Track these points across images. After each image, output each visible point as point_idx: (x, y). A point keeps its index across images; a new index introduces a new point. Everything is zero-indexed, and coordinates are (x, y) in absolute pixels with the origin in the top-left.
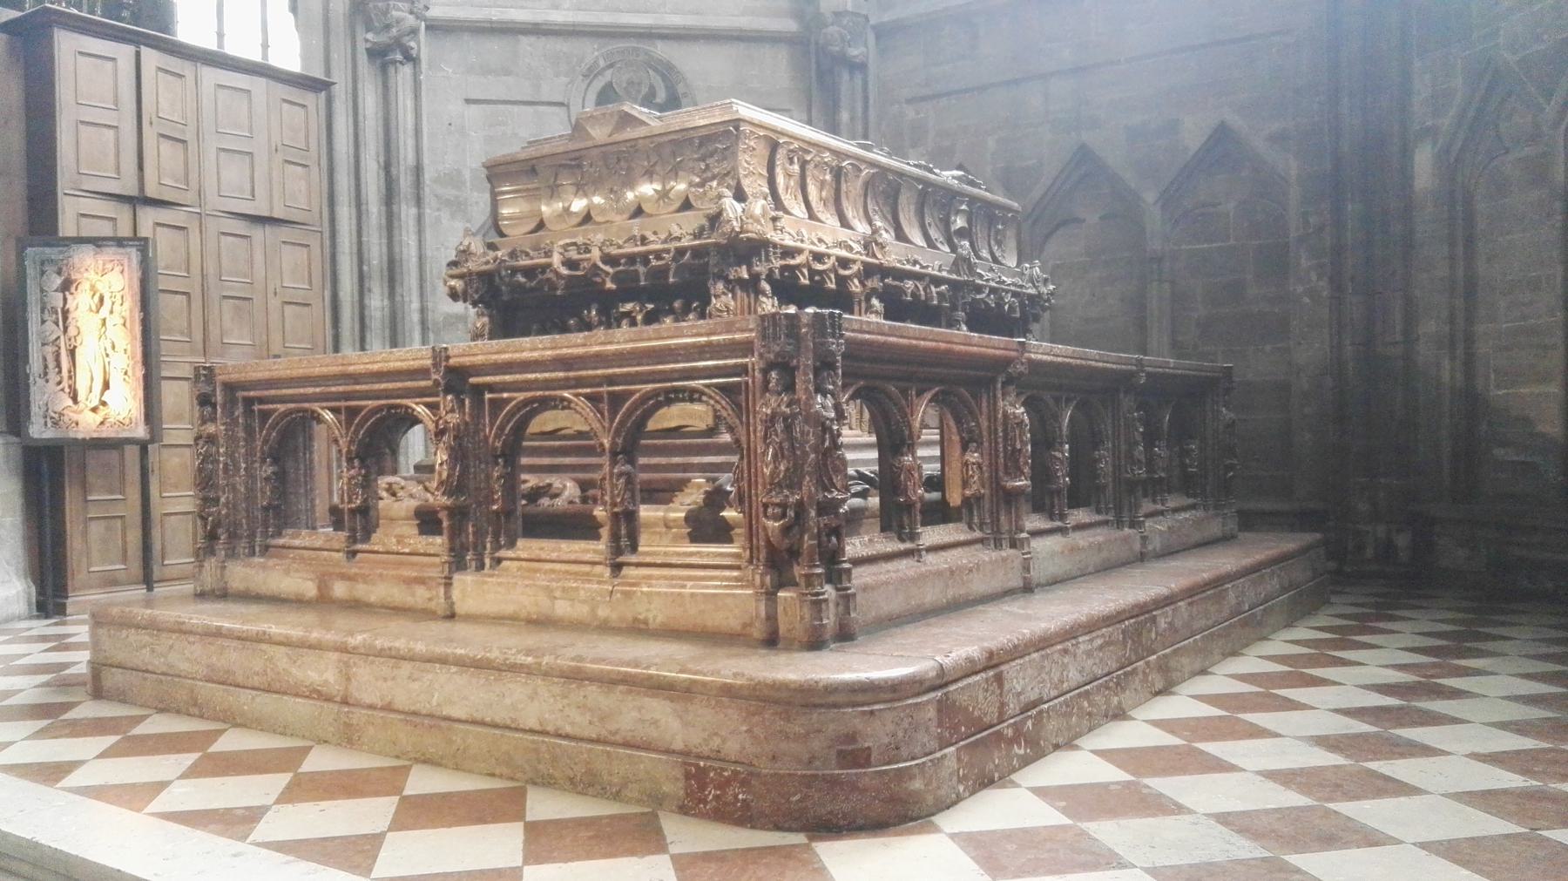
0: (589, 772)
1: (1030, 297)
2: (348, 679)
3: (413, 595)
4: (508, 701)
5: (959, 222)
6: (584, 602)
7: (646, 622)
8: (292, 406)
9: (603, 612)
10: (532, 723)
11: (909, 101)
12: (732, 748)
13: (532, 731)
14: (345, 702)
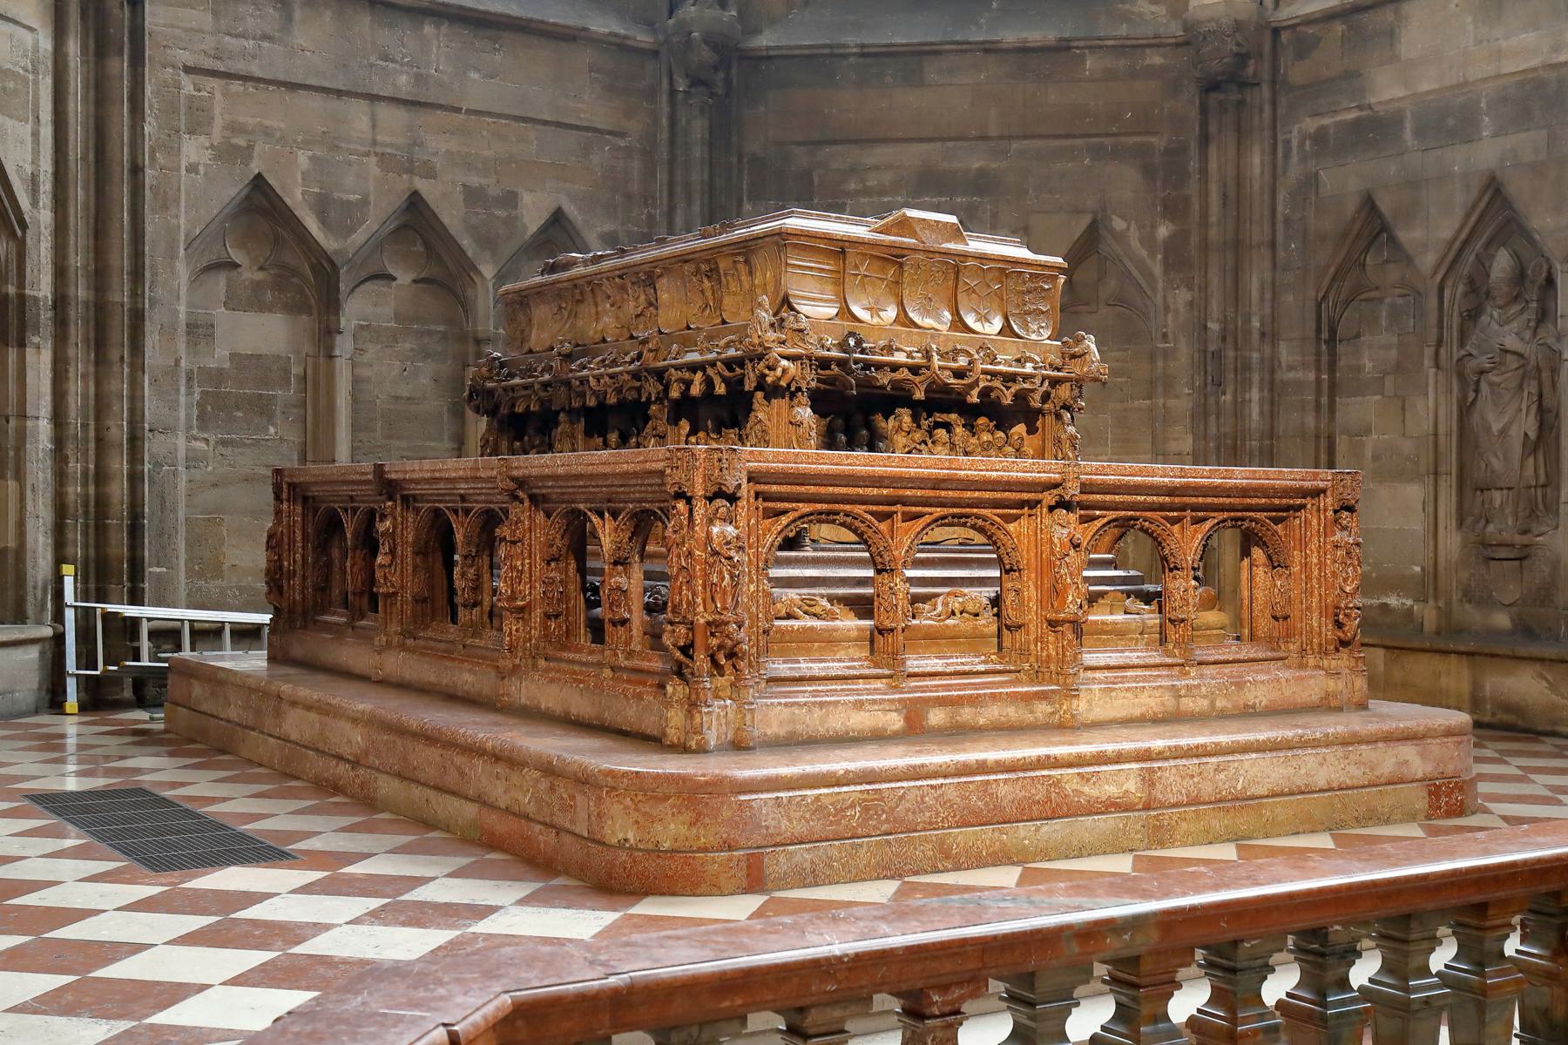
0: (1369, 810)
2: (1152, 784)
3: (1032, 712)
4: (1303, 771)
6: (1205, 697)
7: (1254, 707)
8: (819, 506)
9: (1219, 704)
10: (1322, 783)
11: (188, 70)
12: (1450, 769)
13: (1321, 791)
14: (1147, 808)
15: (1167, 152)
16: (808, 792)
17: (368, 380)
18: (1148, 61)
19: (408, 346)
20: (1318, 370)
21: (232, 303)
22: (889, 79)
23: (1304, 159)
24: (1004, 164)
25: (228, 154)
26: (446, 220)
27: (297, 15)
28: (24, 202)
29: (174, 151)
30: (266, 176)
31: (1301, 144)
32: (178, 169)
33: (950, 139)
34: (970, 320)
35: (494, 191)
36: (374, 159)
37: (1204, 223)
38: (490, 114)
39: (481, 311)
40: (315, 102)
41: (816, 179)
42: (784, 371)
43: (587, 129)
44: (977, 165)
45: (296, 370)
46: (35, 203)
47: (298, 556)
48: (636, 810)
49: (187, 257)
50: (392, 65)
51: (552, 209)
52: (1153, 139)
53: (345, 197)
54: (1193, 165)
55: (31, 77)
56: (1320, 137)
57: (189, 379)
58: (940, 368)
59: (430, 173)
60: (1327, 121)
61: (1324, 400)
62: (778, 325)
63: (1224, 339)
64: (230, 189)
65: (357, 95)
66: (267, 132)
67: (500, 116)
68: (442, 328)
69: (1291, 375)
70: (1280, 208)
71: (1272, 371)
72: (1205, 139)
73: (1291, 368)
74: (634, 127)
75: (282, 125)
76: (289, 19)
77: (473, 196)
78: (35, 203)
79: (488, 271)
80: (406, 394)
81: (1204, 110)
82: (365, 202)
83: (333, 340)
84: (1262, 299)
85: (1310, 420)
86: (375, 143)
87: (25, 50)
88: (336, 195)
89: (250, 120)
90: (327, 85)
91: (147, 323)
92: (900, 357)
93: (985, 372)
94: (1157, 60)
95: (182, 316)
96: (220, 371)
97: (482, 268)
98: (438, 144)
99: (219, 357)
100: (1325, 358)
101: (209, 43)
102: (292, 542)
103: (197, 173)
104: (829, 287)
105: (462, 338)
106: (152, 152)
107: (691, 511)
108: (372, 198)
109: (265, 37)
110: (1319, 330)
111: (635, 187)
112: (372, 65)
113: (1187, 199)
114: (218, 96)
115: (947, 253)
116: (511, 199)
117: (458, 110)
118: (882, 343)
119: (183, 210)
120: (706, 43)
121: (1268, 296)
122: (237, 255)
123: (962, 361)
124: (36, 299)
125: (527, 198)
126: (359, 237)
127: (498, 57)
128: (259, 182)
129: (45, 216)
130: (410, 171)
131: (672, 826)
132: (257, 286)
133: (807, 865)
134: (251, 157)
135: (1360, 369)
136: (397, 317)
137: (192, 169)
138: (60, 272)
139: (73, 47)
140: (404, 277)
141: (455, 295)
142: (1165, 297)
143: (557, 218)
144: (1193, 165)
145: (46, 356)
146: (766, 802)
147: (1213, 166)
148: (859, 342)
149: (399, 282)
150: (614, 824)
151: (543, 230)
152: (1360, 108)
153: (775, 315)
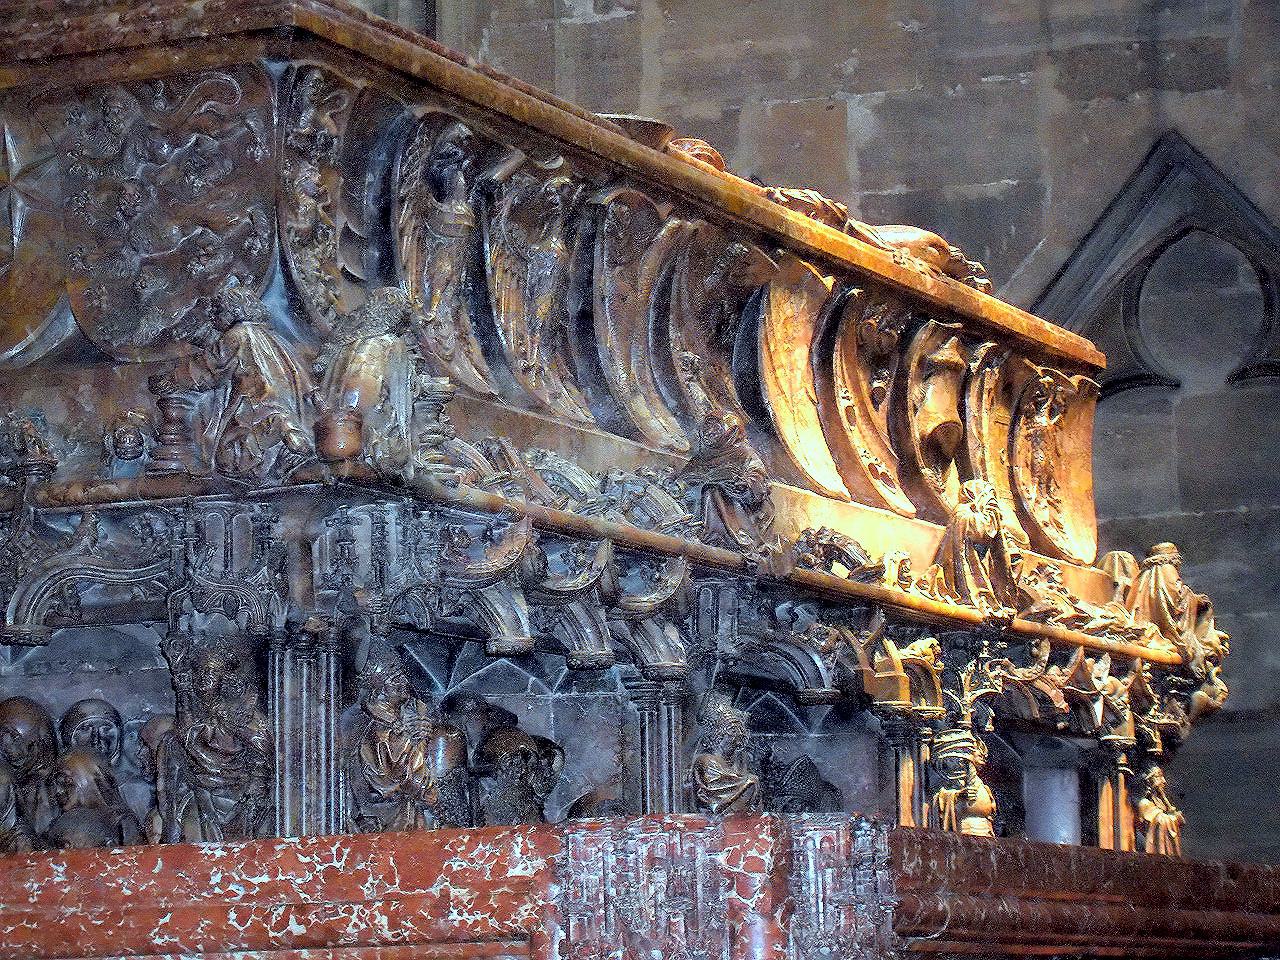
1: (1159, 668)
5: (932, 406)
36: (1049, 73)
53: (973, 191)
59: (1209, 71)
66: (770, 71)
75: (806, 42)
82: (1028, 195)
86: (1046, 26)
89: (728, 51)
108: (1048, 181)
130: (1154, 81)
140: (1203, 378)
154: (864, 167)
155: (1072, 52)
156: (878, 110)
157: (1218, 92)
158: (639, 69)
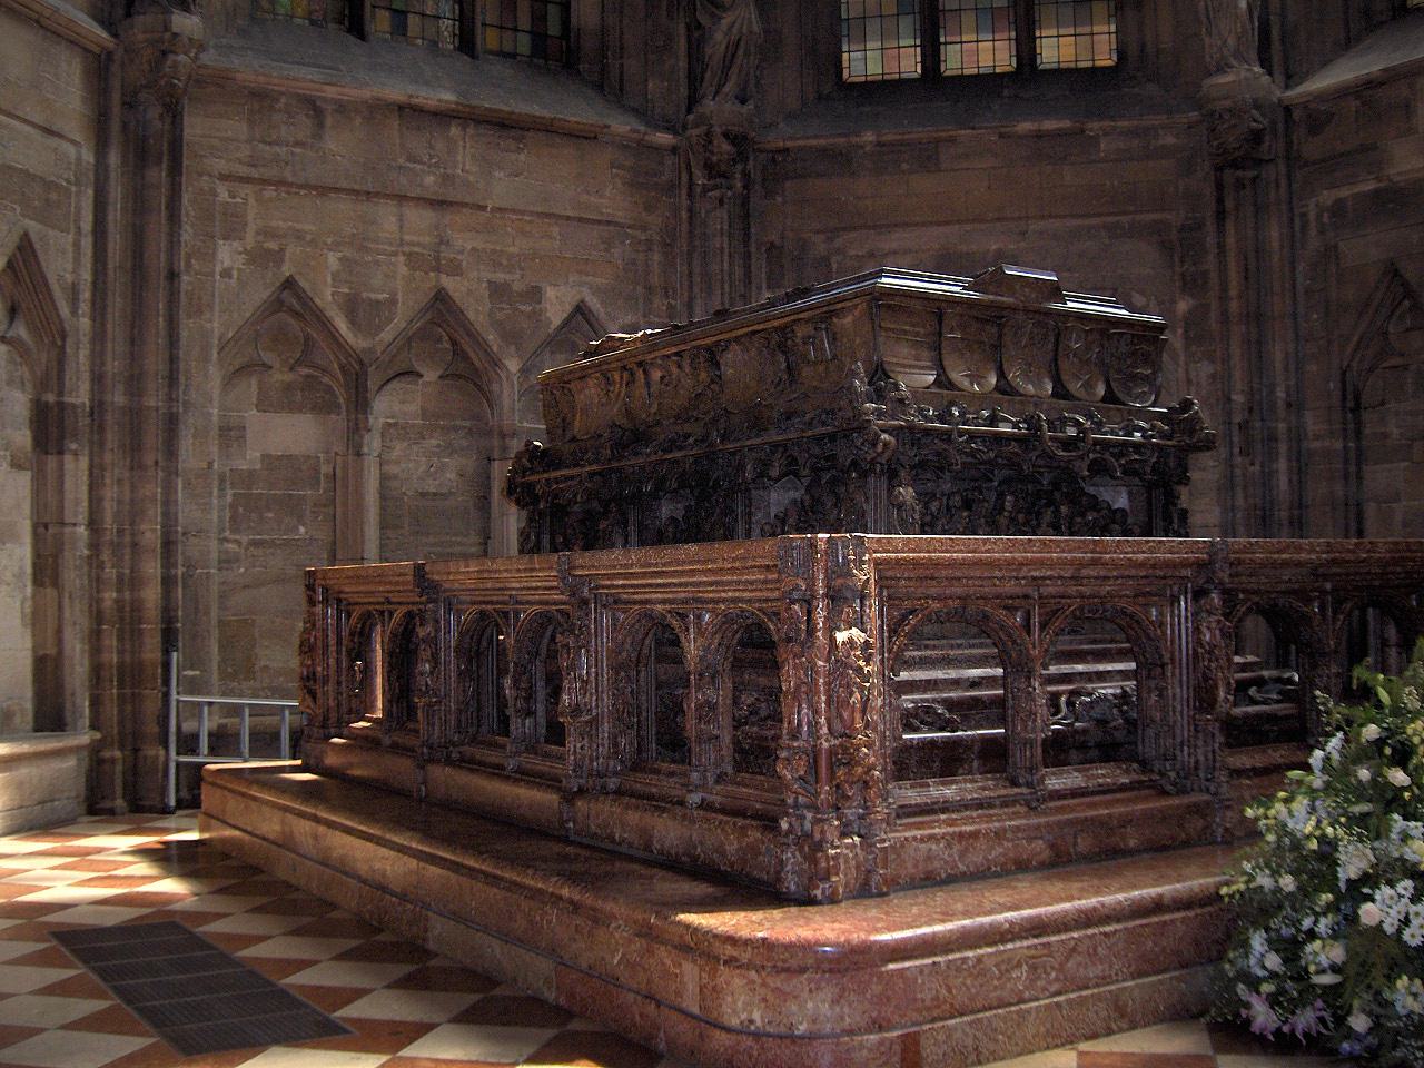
11: (224, 178)
15: (1182, 229)
16: (970, 954)
17: (396, 477)
18: (1161, 142)
19: (434, 442)
20: (1345, 438)
21: (263, 405)
22: (905, 166)
23: (1322, 232)
24: (1023, 244)
25: (261, 258)
26: (471, 316)
27: (329, 121)
28: (65, 311)
29: (211, 257)
30: (297, 278)
31: (1319, 217)
32: (212, 274)
33: (968, 221)
34: (1075, 387)
35: (517, 287)
36: (401, 259)
37: (1224, 297)
38: (514, 211)
39: (506, 402)
40: (343, 206)
41: (835, 266)
42: (886, 444)
43: (608, 223)
44: (994, 247)
45: (325, 469)
46: (74, 312)
47: (332, 661)
48: (764, 984)
49: (220, 360)
50: (419, 167)
51: (575, 303)
52: (1167, 216)
53: (373, 296)
54: (1211, 241)
55: (73, 189)
56: (1338, 209)
57: (222, 480)
58: (1051, 438)
59: (456, 270)
60: (1344, 192)
61: (1353, 469)
62: (879, 396)
63: (1251, 410)
64: (260, 294)
65: (387, 196)
66: (299, 236)
67: (523, 213)
68: (468, 424)
69: (1316, 445)
70: (1300, 280)
71: (1299, 441)
72: (1221, 215)
73: (1317, 437)
74: (655, 220)
76: (321, 125)
77: (498, 291)
78: (74, 312)
79: (513, 365)
80: (432, 490)
81: (1219, 186)
82: (393, 302)
83: (362, 437)
84: (1286, 369)
85: (1339, 490)
86: (402, 242)
87: (70, 163)
88: (364, 295)
90: (356, 187)
91: (182, 426)
92: (1004, 428)
93: (1097, 442)
94: (1170, 140)
95: (215, 419)
96: (251, 473)
97: (507, 362)
98: (464, 242)
99: (249, 458)
100: (1351, 426)
101: (244, 152)
102: (326, 647)
103: (230, 277)
104: (926, 353)
105: (489, 433)
106: (189, 256)
107: (809, 613)
108: (400, 297)
109: (297, 144)
110: (1344, 398)
111: (656, 280)
112: (400, 167)
113: (1205, 274)
114: (252, 201)
115: (1050, 313)
116: (535, 294)
117: (483, 208)
118: (985, 413)
119: (217, 314)
120: (726, 135)
121: (1292, 367)
122: (268, 357)
123: (1071, 431)
124: (74, 406)
125: (550, 293)
126: (387, 335)
127: (522, 157)
128: (289, 284)
129: (85, 323)
130: (438, 270)
131: (810, 1005)
132: (288, 388)
133: (969, 1042)
134: (282, 260)
135: (1385, 436)
136: (424, 414)
137: (226, 273)
138: (98, 379)
139: (114, 158)
140: (431, 375)
141: (480, 389)
142: (1187, 371)
143: (581, 310)
144: (1211, 241)
145: (84, 462)
146: (921, 970)
147: (1231, 241)
148: (962, 414)
149: (426, 379)
150: (735, 1002)
151: (566, 323)
152: (1379, 179)
153: (870, 384)
154: (333, 280)
155: (410, 254)
156: (340, 259)
157: (458, 278)
158: (246, 224)
